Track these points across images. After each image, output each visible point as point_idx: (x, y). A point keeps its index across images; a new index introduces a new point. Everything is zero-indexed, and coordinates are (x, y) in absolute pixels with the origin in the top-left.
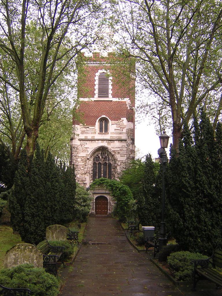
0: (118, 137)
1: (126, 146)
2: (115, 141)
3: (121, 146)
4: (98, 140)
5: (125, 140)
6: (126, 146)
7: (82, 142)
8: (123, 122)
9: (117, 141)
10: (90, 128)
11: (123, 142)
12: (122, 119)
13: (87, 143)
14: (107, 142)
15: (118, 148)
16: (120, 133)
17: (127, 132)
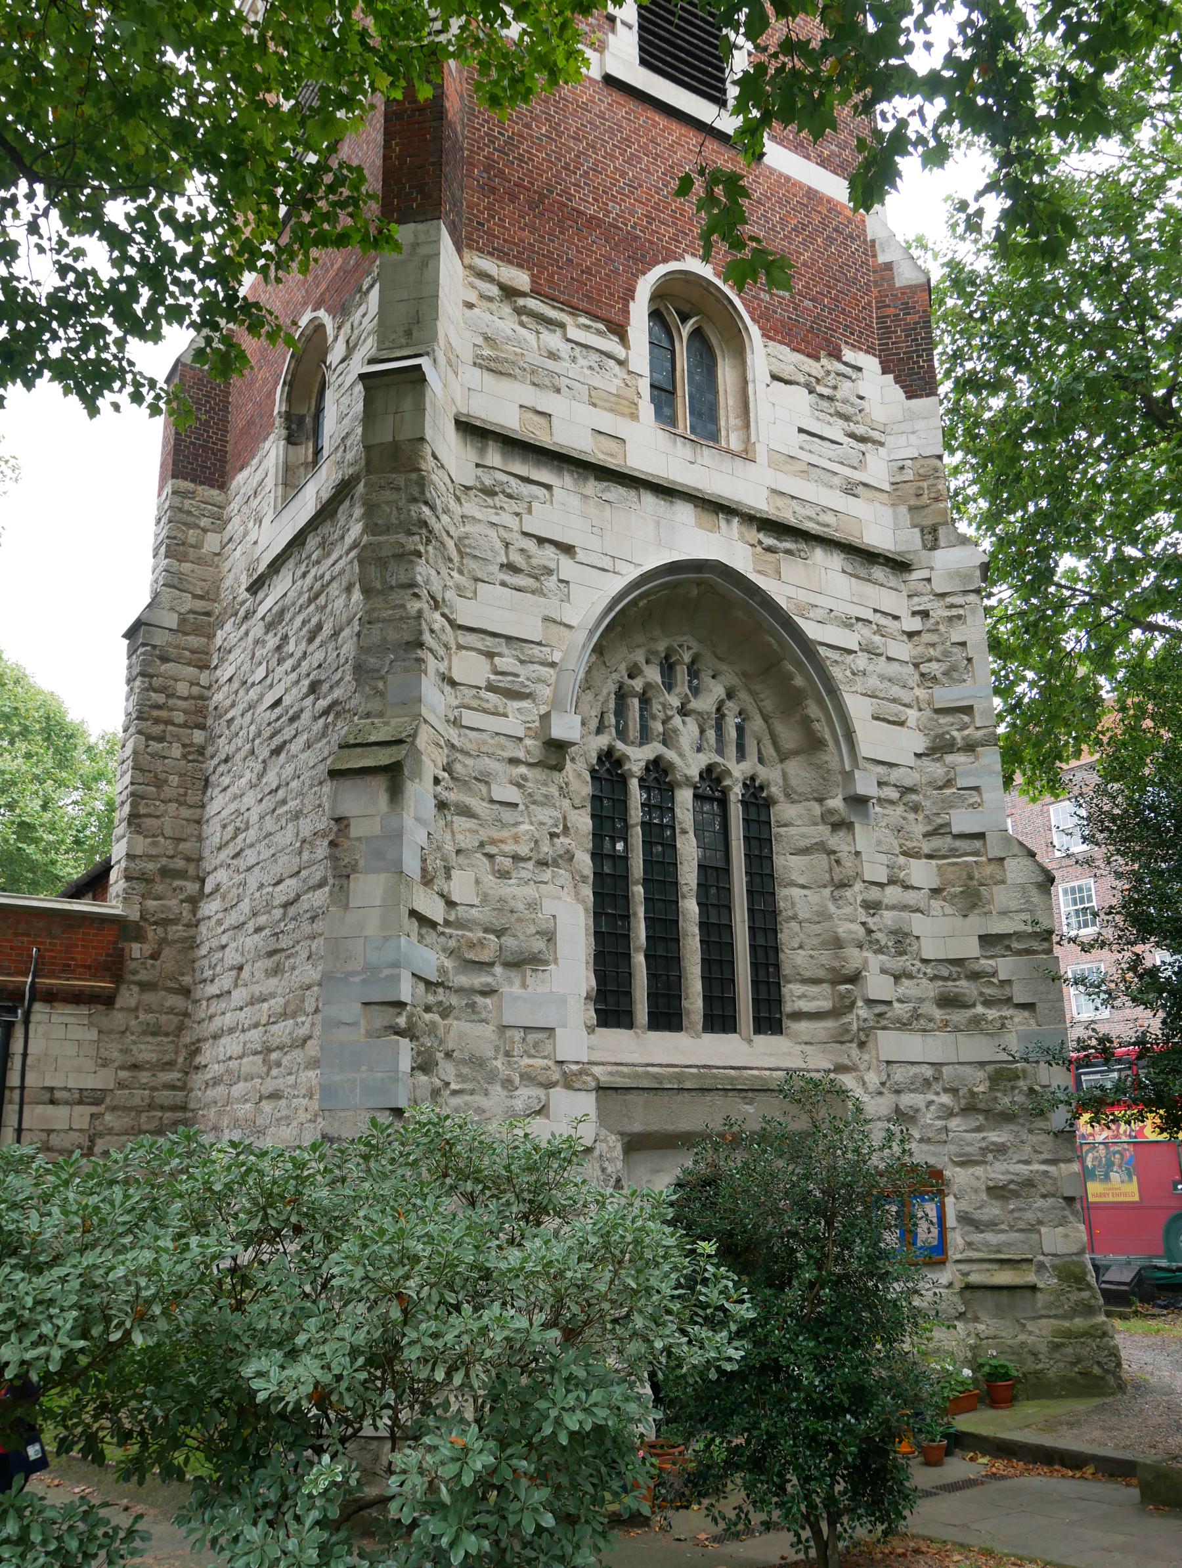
0: (829, 518)
1: (915, 624)
2: (819, 554)
3: (868, 614)
4: (666, 491)
5: (899, 566)
6: (915, 624)
7: (494, 457)
8: (863, 388)
9: (836, 560)
10: (573, 333)
11: (878, 572)
12: (849, 355)
13: (549, 487)
14: (754, 535)
15: (849, 623)
16: (851, 489)
17: (910, 489)
